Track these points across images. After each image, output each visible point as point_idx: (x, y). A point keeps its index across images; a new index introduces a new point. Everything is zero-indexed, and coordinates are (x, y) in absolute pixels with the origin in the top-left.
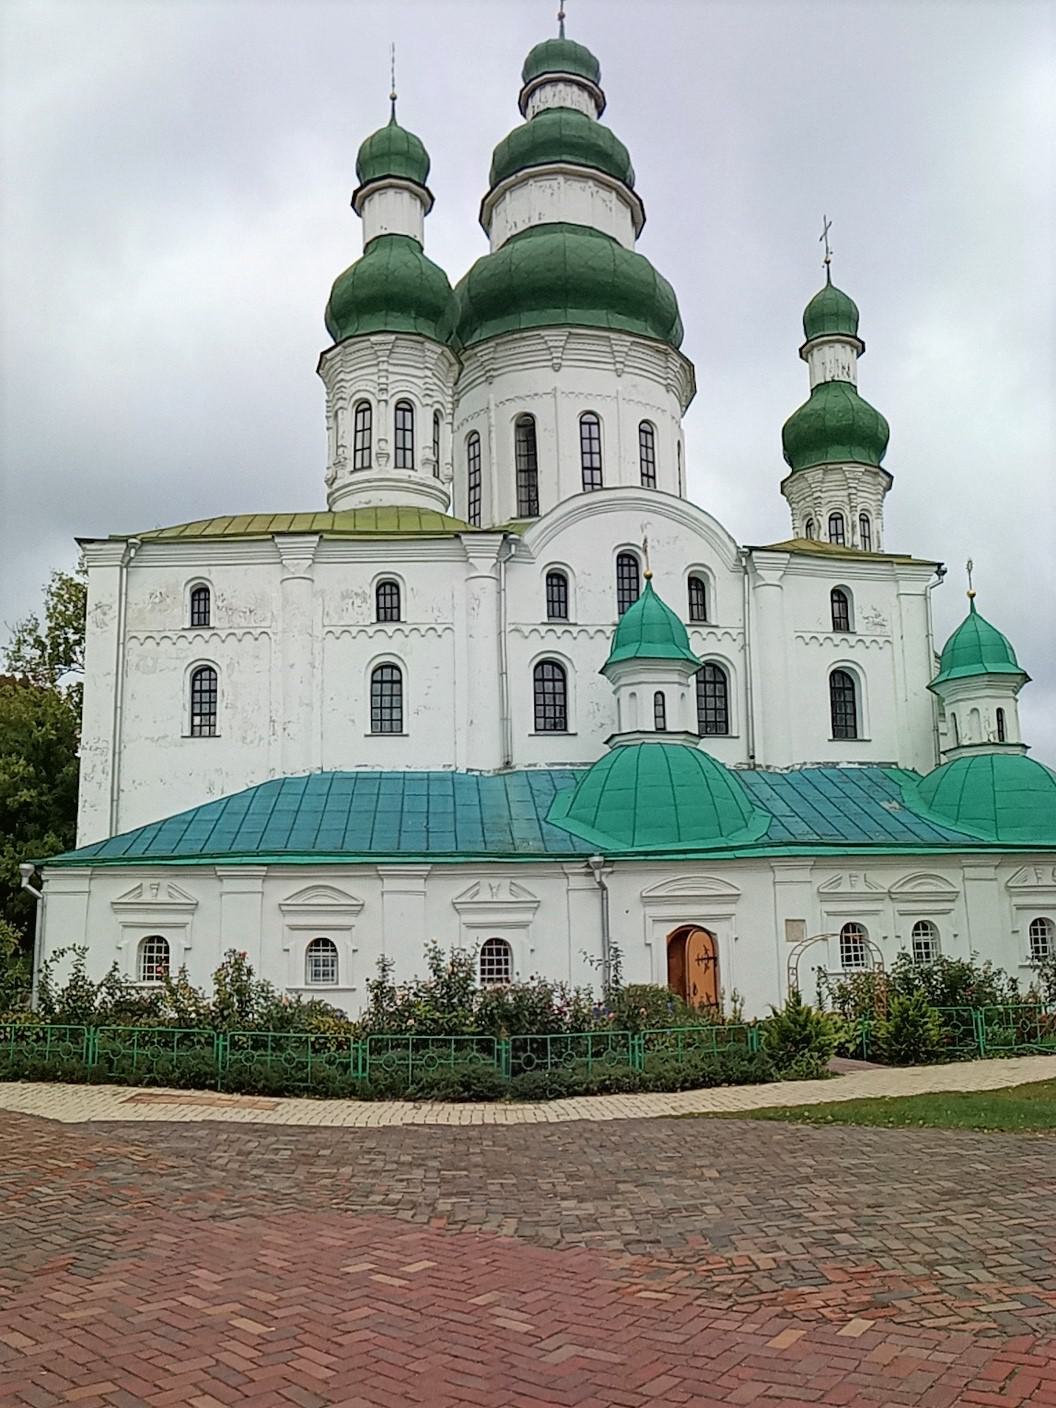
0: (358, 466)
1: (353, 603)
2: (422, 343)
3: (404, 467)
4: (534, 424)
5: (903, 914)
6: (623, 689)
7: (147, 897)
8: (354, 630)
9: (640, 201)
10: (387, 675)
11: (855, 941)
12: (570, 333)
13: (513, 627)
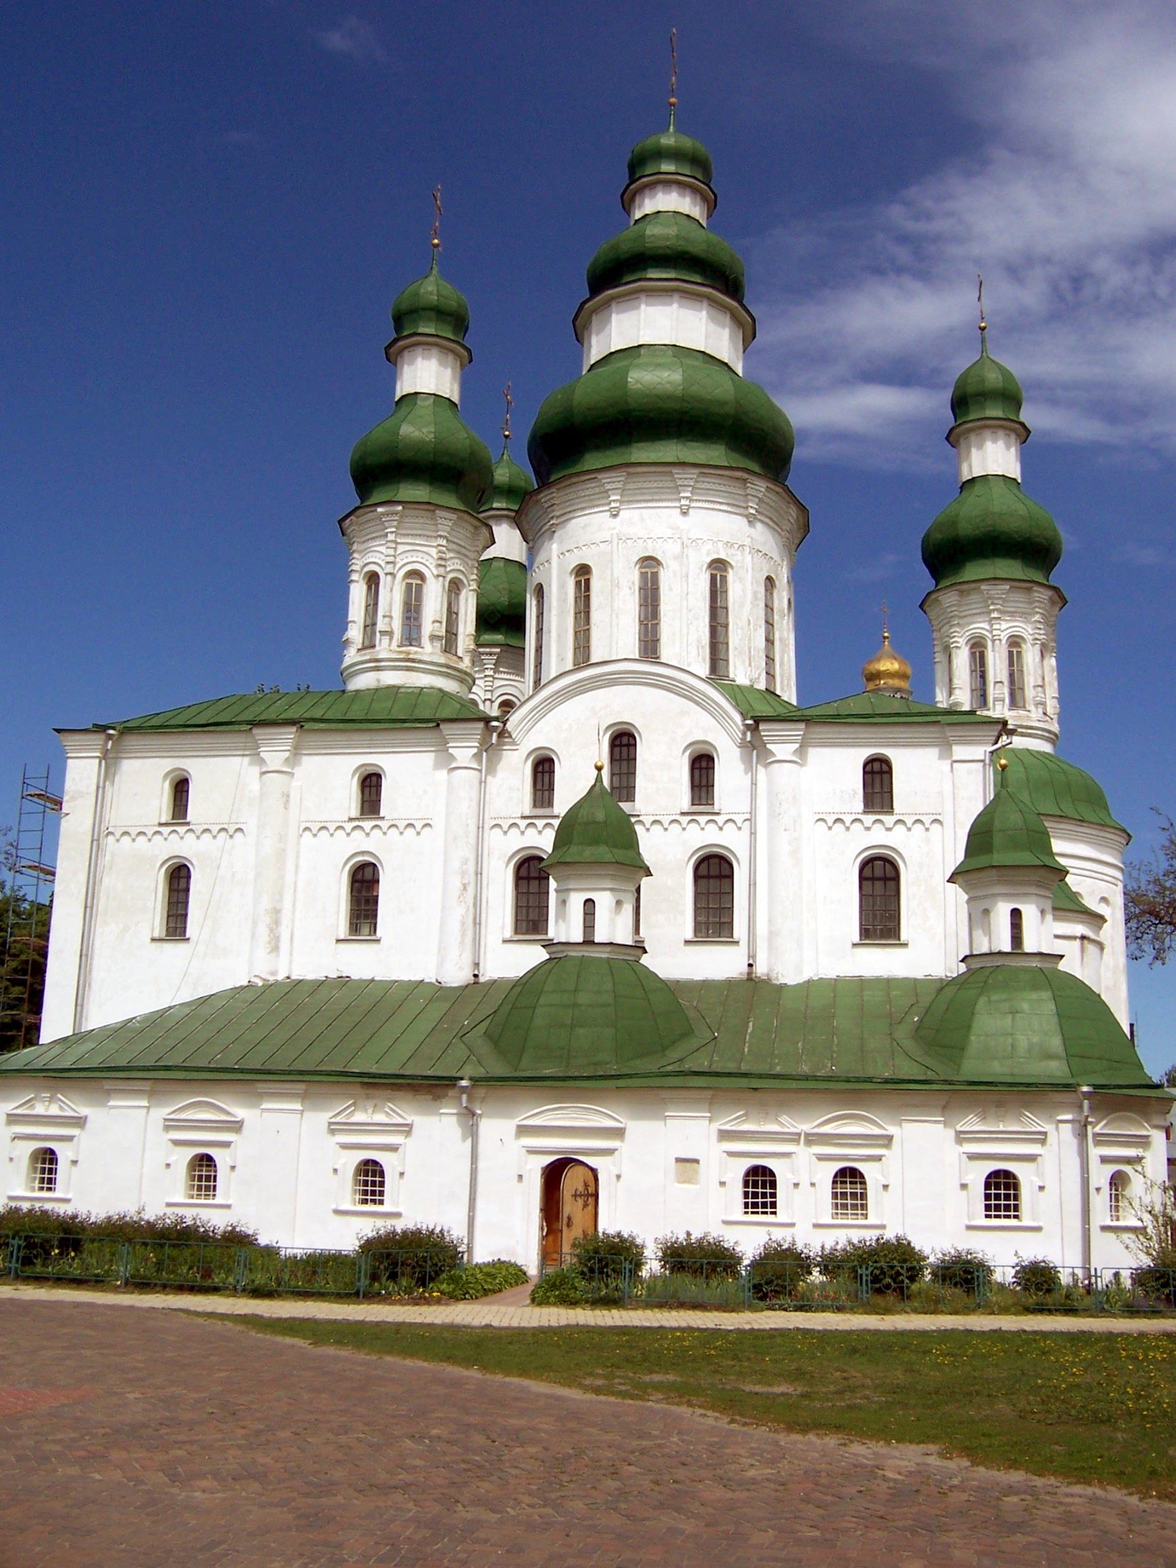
2: (434, 511)
5: (822, 1158)
10: (368, 873)
11: (764, 1187)
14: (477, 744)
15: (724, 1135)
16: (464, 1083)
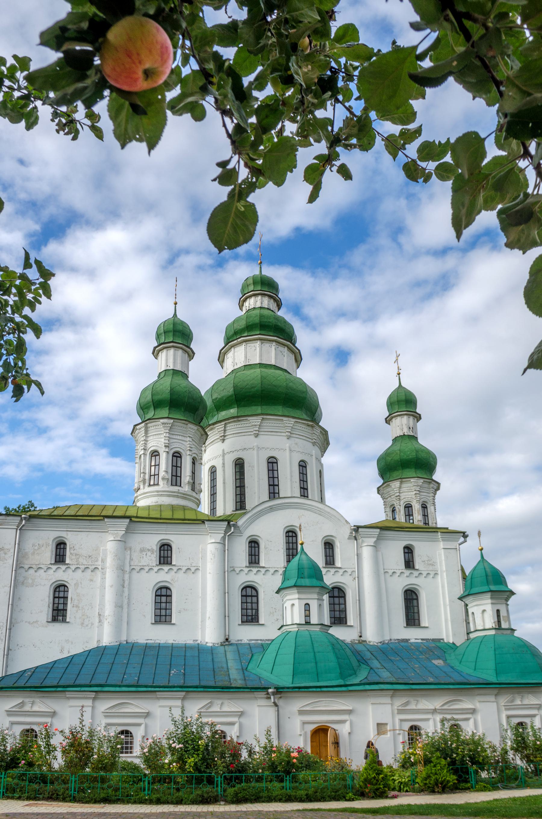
0: (152, 483)
1: (146, 554)
3: (176, 485)
4: (244, 463)
6: (288, 602)
7: (27, 708)
8: (147, 569)
9: (299, 350)
12: (263, 418)
13: (232, 569)
14: (223, 532)
15: (400, 712)
16: (270, 690)
